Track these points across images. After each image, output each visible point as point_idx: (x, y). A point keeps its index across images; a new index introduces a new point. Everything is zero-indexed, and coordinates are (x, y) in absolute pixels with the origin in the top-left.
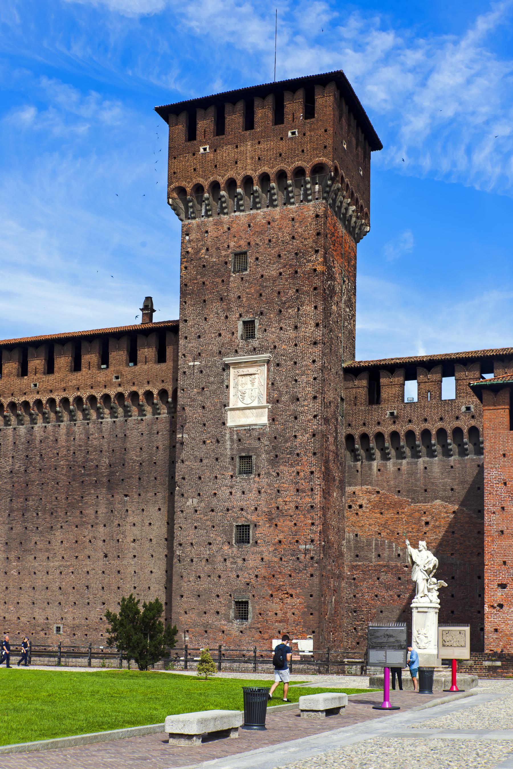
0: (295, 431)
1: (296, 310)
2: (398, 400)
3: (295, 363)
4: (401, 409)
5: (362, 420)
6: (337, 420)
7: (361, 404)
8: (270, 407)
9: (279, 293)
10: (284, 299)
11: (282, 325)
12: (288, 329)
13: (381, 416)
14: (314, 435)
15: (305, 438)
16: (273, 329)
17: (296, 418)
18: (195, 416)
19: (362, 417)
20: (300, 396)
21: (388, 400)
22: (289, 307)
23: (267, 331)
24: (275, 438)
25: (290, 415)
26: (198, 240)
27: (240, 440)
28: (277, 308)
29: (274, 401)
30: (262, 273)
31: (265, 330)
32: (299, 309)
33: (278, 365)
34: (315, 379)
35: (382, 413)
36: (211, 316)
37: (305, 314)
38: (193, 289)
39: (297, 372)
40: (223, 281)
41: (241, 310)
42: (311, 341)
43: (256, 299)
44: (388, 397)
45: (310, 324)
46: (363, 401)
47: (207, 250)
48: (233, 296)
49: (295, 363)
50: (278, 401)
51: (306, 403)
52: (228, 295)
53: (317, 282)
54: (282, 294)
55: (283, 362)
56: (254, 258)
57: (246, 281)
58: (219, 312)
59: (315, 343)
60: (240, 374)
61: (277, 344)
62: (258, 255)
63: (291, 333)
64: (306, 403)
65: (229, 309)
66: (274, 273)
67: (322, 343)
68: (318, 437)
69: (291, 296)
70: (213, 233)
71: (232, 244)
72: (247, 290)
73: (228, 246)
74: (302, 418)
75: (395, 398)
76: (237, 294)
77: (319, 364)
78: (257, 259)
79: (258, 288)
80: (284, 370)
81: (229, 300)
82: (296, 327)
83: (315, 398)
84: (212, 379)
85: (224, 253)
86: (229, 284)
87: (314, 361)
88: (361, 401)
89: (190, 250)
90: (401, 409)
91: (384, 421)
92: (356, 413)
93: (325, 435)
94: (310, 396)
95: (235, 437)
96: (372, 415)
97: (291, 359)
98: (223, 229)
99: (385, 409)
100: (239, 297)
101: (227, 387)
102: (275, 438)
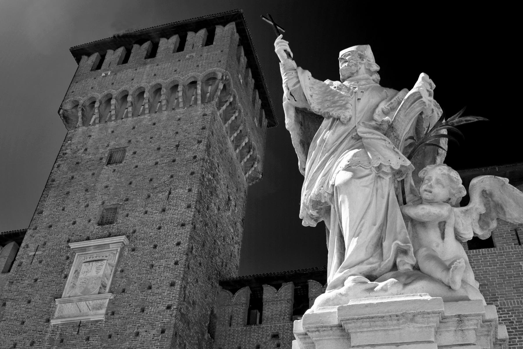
0: (139, 327)
1: (167, 194)
2: (284, 319)
3: (155, 247)
4: (288, 329)
5: (237, 343)
6: (203, 335)
7: (237, 324)
8: (112, 298)
9: (151, 180)
10: (155, 185)
11: (147, 209)
12: (154, 212)
13: (262, 338)
14: (163, 332)
15: (151, 335)
16: (137, 214)
17: (143, 310)
18: (15, 312)
19: (237, 339)
20: (153, 283)
21: (272, 319)
22: (158, 192)
23: (130, 215)
24: (110, 337)
25: (137, 306)
26: (79, 143)
27: (62, 341)
28: (146, 193)
29: (118, 290)
30: (137, 164)
31: (127, 215)
32: (170, 193)
33: (133, 250)
34: (176, 263)
35: (263, 335)
36: (71, 205)
37: (177, 197)
38: (59, 183)
39: (156, 255)
40: (93, 174)
41: (106, 197)
42: (178, 223)
43: (124, 186)
44: (272, 315)
45: (181, 206)
46: (240, 320)
47: (86, 150)
48: (99, 186)
49: (155, 247)
50: (124, 291)
51: (160, 291)
52: (95, 185)
53: (196, 167)
54: (154, 180)
55: (141, 246)
56: (131, 153)
57: (118, 171)
58: (81, 201)
59: (183, 225)
60: (86, 260)
61: (137, 228)
62: (136, 150)
63: (158, 217)
64: (160, 291)
65: (93, 198)
66: (151, 163)
67: (192, 224)
68: (169, 333)
69: (164, 182)
70: (94, 135)
71: (112, 143)
72: (117, 180)
73: (108, 146)
74: (150, 310)
75: (280, 315)
76: (104, 184)
77: (185, 246)
78: (135, 153)
79: (130, 177)
80: (140, 255)
81: (95, 190)
82: (164, 210)
83: (172, 284)
84: (51, 269)
85: (101, 150)
86: (99, 176)
87: (178, 244)
88: (238, 320)
89: (67, 151)
90: (288, 329)
91: (265, 343)
92: (229, 335)
93: (180, 336)
94: (167, 283)
95: (57, 337)
96: (250, 337)
97: (151, 243)
98: (107, 131)
99: (267, 329)
100: (107, 187)
101: (66, 277)
102: (110, 337)
